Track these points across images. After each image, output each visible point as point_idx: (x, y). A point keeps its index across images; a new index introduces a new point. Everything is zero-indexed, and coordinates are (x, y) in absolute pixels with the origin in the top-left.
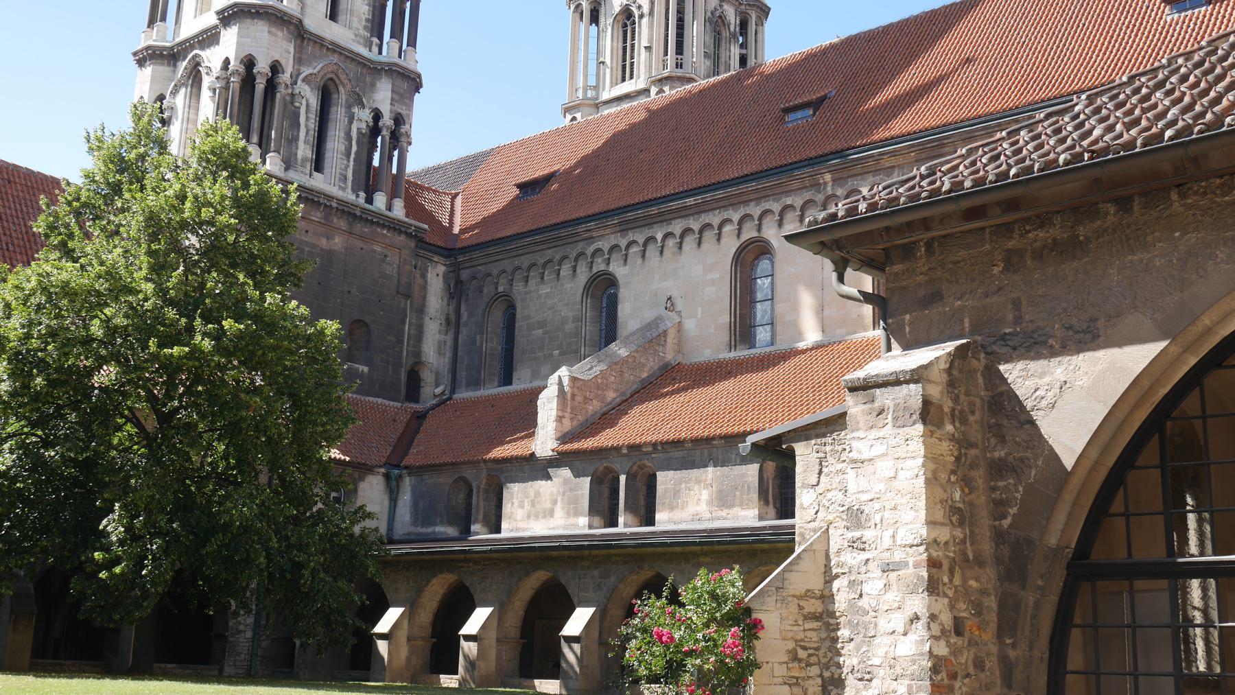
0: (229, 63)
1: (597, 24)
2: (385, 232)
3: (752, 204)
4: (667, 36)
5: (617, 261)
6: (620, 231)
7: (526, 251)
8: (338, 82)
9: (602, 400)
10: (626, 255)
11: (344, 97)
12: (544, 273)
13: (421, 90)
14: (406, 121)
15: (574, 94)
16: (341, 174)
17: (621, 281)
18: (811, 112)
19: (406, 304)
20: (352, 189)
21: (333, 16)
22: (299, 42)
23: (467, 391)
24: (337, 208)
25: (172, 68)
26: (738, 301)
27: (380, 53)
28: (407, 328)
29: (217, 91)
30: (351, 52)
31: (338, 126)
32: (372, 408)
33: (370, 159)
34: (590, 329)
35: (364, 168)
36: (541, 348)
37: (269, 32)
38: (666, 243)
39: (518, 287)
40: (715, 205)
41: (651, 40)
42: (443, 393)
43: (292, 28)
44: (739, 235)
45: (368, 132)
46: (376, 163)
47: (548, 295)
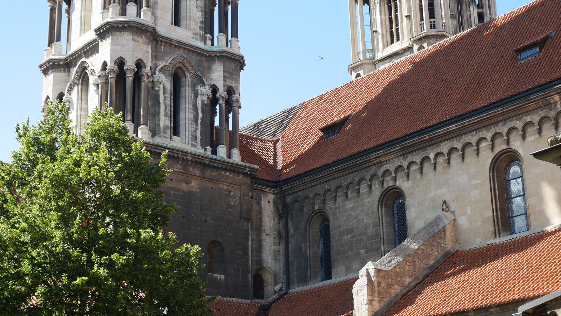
0: (107, 65)
1: (368, 4)
2: (228, 174)
3: (501, 124)
4: (421, 6)
5: (401, 178)
6: (402, 155)
7: (332, 177)
8: (184, 69)
9: (402, 284)
10: (408, 173)
11: (190, 79)
12: (347, 192)
13: (244, 68)
14: (236, 91)
15: (356, 57)
16: (192, 135)
17: (406, 192)
18: (538, 50)
20: (201, 145)
21: (177, 22)
22: (154, 44)
23: (298, 286)
24: (192, 160)
25: (67, 73)
26: (498, 199)
27: (213, 44)
28: (250, 244)
29: (100, 86)
30: (192, 46)
31: (187, 101)
32: (229, 306)
33: (212, 122)
34: (386, 231)
35: (208, 129)
36: (351, 249)
37: (133, 40)
38: (438, 160)
39: (330, 204)
40: (472, 128)
41: (409, 10)
42: (281, 289)
43: (148, 34)
44: (492, 149)
45: (209, 102)
46: (217, 123)
47: (352, 209)
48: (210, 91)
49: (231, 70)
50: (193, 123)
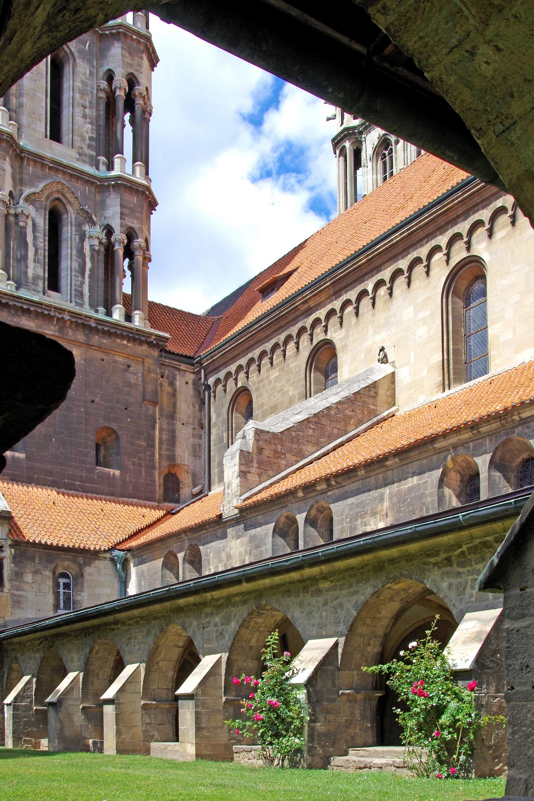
2: (125, 342)
5: (334, 326)
8: (64, 201)
11: (73, 216)
16: (76, 290)
17: (338, 345)
19: (154, 411)
47: (277, 379)
48: (104, 234)
49: (132, 206)
50: (78, 275)
